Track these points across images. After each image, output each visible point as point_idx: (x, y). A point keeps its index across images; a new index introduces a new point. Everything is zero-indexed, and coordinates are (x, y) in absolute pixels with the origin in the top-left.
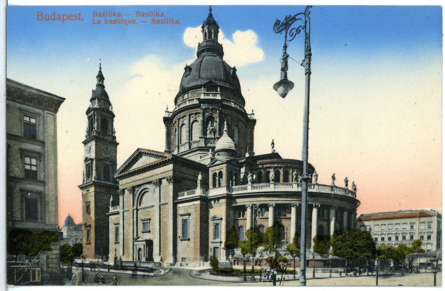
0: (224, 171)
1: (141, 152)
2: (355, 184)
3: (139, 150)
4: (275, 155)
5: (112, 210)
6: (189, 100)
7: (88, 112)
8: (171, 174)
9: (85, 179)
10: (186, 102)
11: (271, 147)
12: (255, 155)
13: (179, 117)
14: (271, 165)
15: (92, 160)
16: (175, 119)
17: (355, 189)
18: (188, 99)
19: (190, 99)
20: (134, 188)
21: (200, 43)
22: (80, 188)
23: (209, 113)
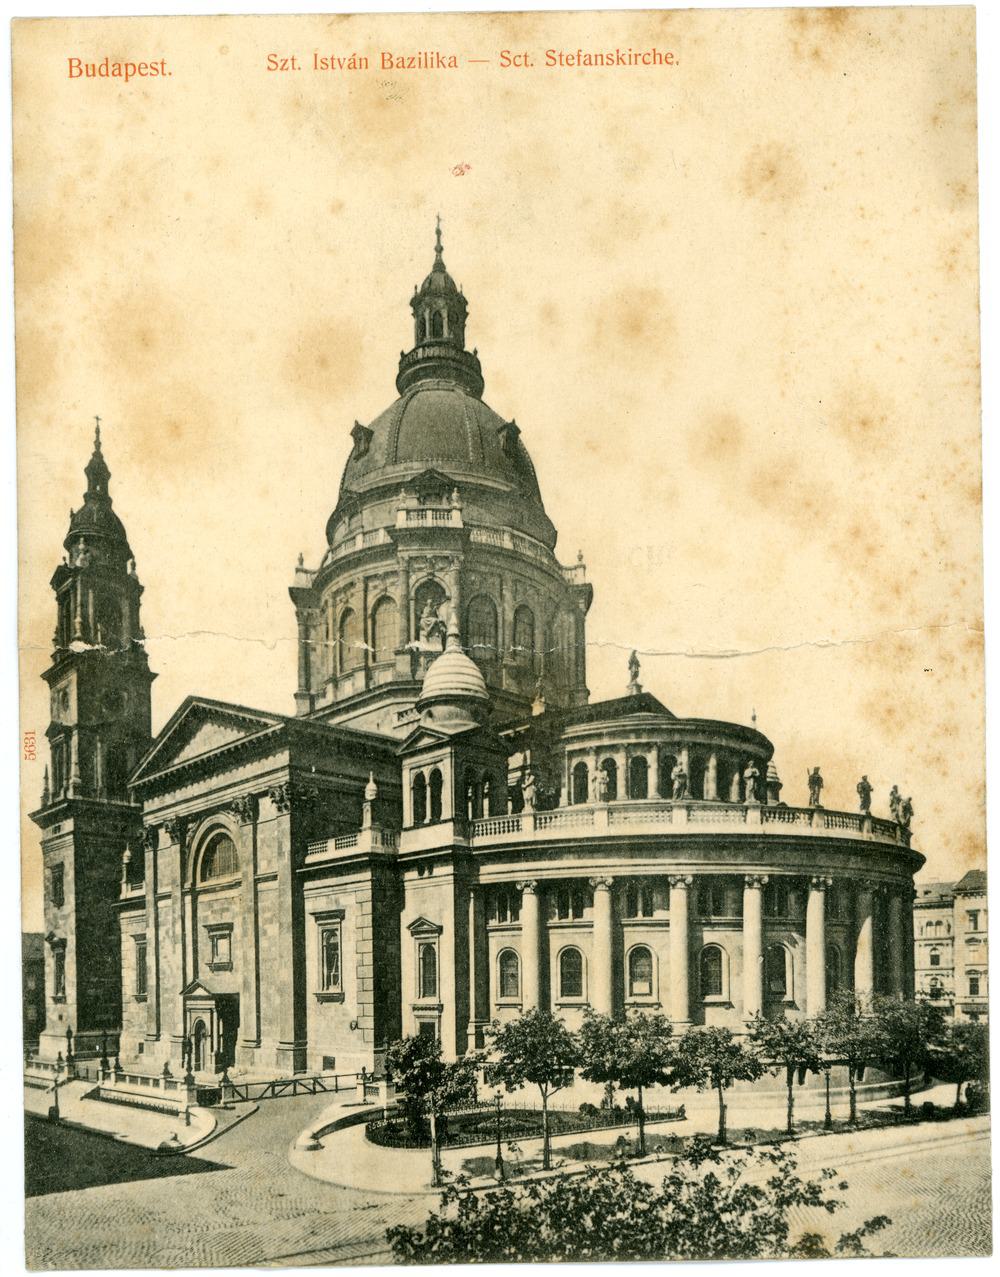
0: (447, 770)
2: (904, 795)
4: (643, 702)
5: (127, 892)
6: (364, 534)
8: (284, 777)
10: (354, 538)
11: (627, 675)
12: (592, 700)
13: (334, 589)
15: (68, 731)
16: (326, 595)
17: (908, 810)
19: (366, 530)
21: (406, 352)
23: (425, 574)
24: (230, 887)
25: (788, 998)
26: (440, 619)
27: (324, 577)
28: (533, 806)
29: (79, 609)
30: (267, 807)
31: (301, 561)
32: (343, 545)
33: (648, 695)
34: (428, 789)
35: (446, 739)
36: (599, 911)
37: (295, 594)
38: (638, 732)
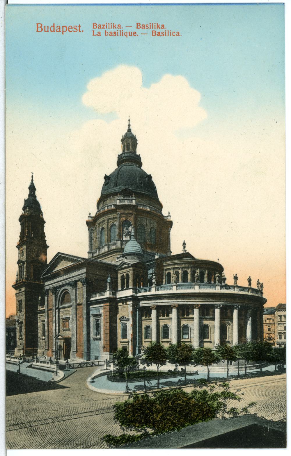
1: (60, 255)
2: (261, 282)
4: (187, 255)
5: (40, 308)
8: (84, 276)
10: (105, 207)
11: (182, 247)
12: (172, 254)
13: (99, 222)
14: (171, 267)
15: (23, 262)
17: (262, 286)
18: (107, 205)
19: (108, 205)
24: (68, 307)
25: (227, 340)
26: (129, 231)
28: (155, 285)
29: (27, 227)
30: (80, 284)
31: (90, 214)
33: (188, 253)
34: (125, 279)
35: (131, 265)
36: (174, 314)
37: (88, 223)
38: (185, 264)
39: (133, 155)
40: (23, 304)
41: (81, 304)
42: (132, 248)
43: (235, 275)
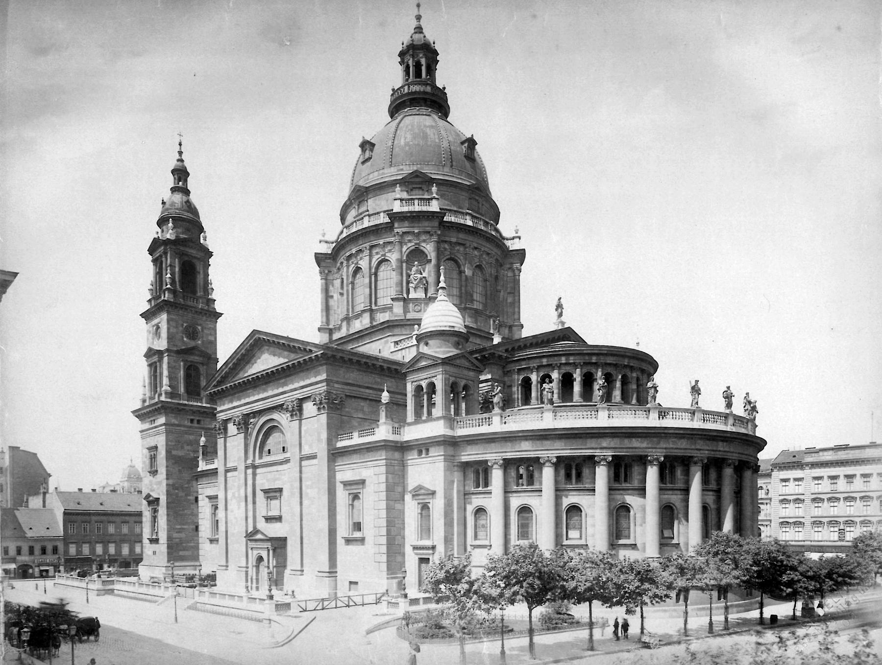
2: (752, 398)
3: (255, 335)
5: (202, 466)
7: (151, 251)
8: (322, 388)
9: (148, 395)
10: (363, 218)
13: (348, 254)
15: (160, 353)
17: (754, 409)
18: (367, 213)
20: (247, 417)
22: (136, 416)
23: (413, 244)
25: (675, 541)
27: (341, 246)
28: (500, 408)
29: (169, 268)
30: (309, 408)
32: (355, 224)
33: (569, 329)
37: (320, 259)
38: (567, 355)
39: (429, 89)
40: (162, 456)
41: (313, 457)
42: (439, 318)
43: (693, 384)
